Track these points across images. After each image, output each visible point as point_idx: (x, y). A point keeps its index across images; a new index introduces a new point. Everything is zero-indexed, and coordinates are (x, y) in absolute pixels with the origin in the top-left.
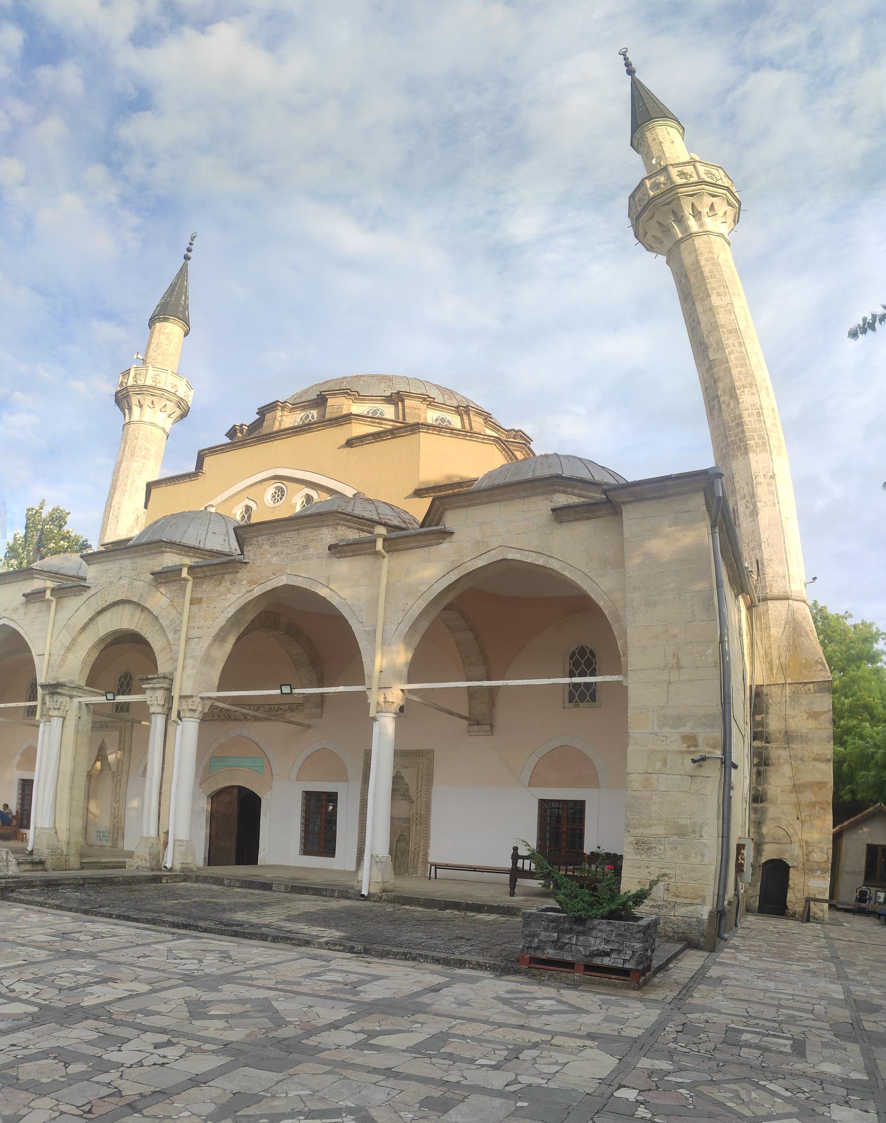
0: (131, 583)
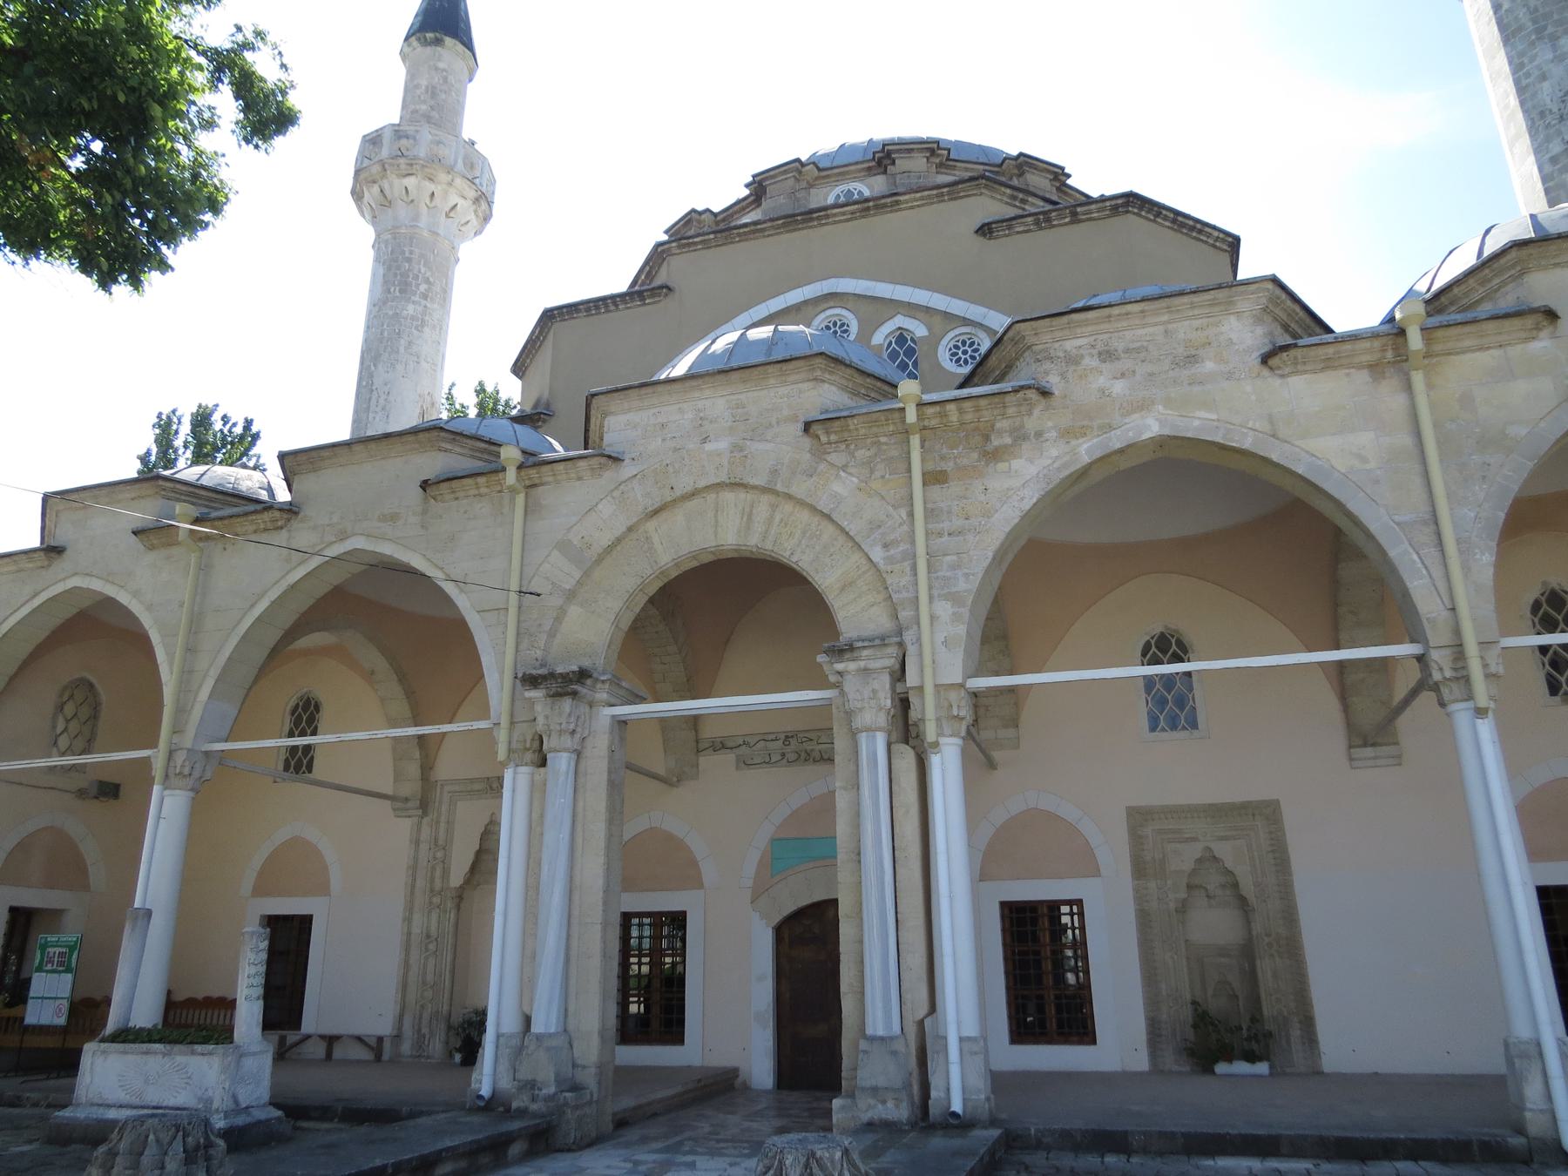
0: (737, 448)
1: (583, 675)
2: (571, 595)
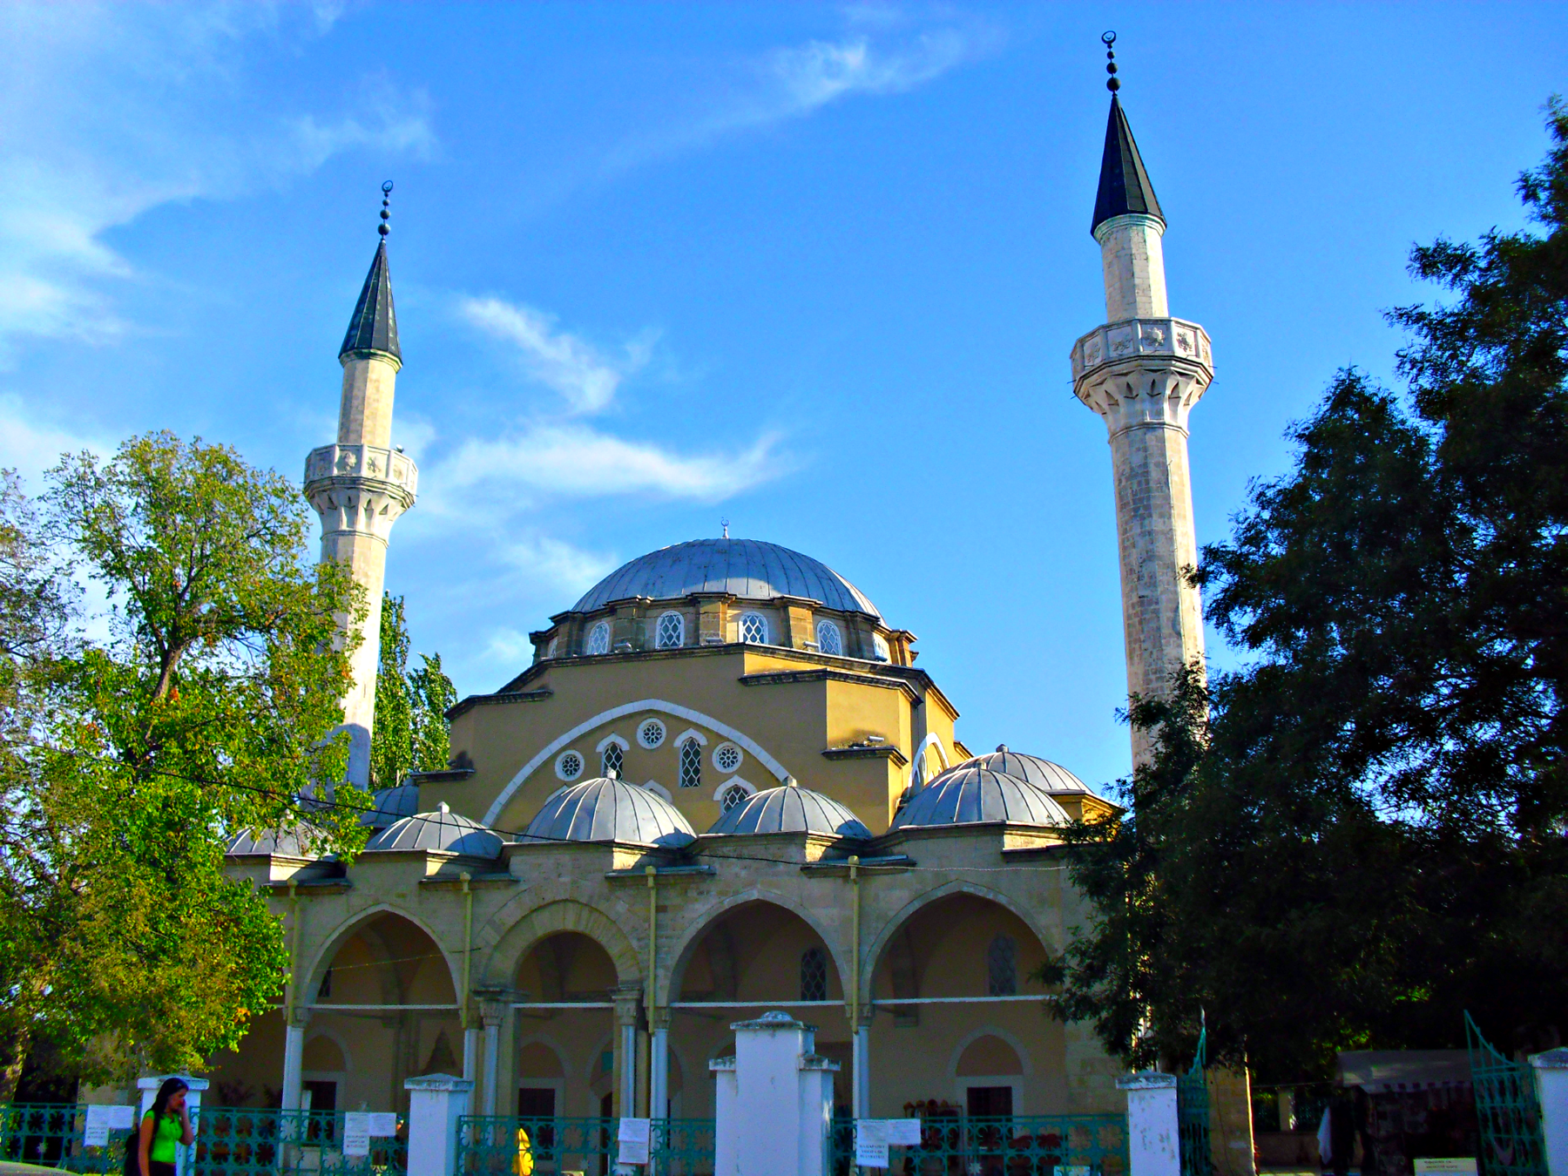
0: (574, 882)
2: (497, 947)
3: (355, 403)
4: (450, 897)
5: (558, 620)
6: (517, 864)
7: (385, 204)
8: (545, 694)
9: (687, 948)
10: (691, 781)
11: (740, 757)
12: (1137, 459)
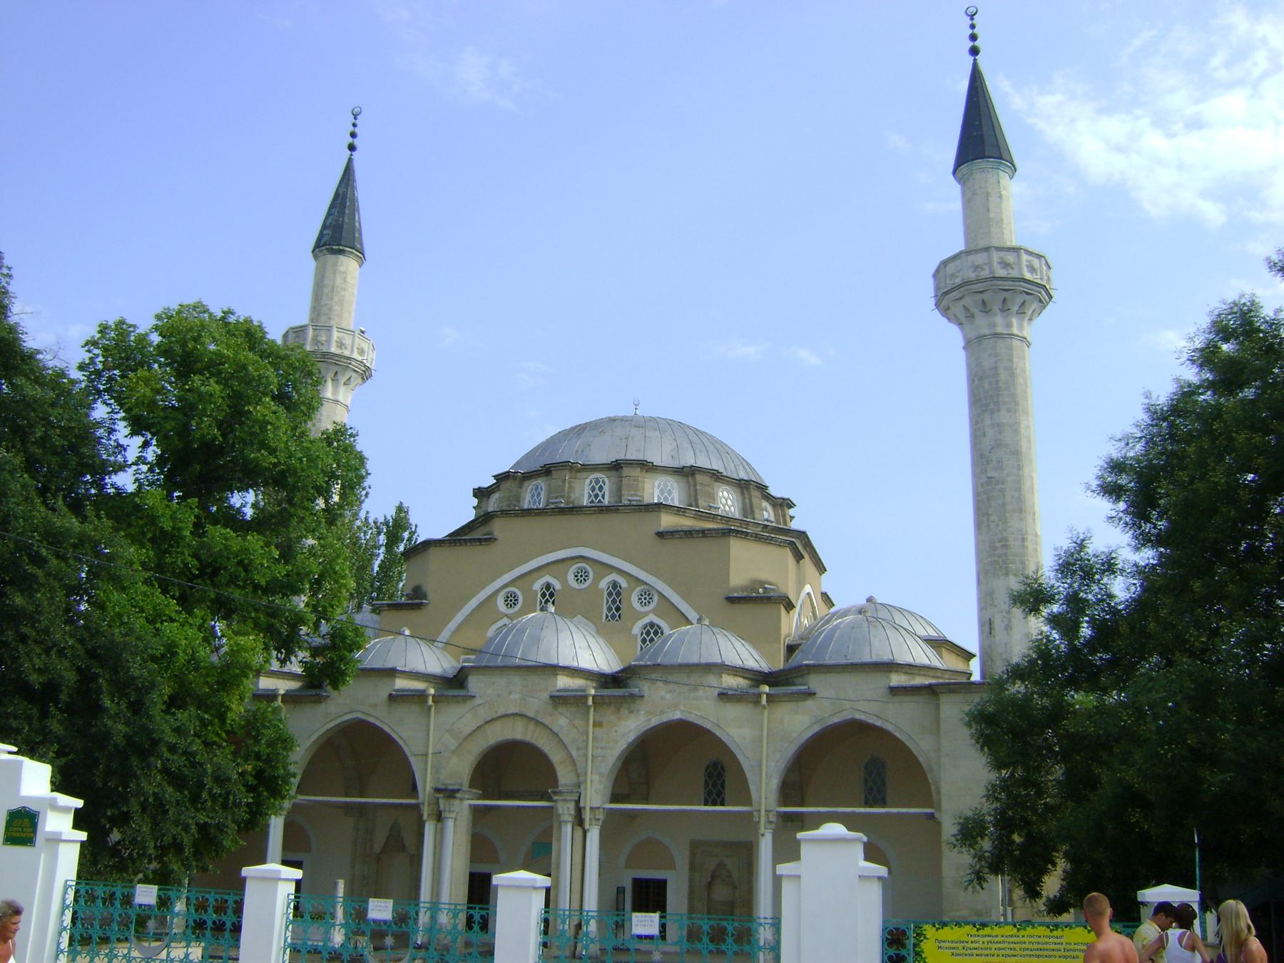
0: (523, 699)
1: (458, 790)
2: (454, 752)
3: (326, 290)
4: (415, 708)
5: (502, 478)
6: (474, 683)
7: (354, 125)
8: (489, 540)
9: (620, 756)
10: (613, 617)
11: (656, 598)
12: (988, 363)
